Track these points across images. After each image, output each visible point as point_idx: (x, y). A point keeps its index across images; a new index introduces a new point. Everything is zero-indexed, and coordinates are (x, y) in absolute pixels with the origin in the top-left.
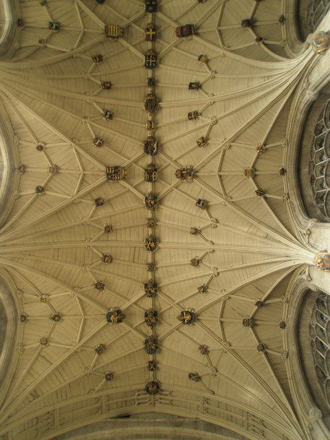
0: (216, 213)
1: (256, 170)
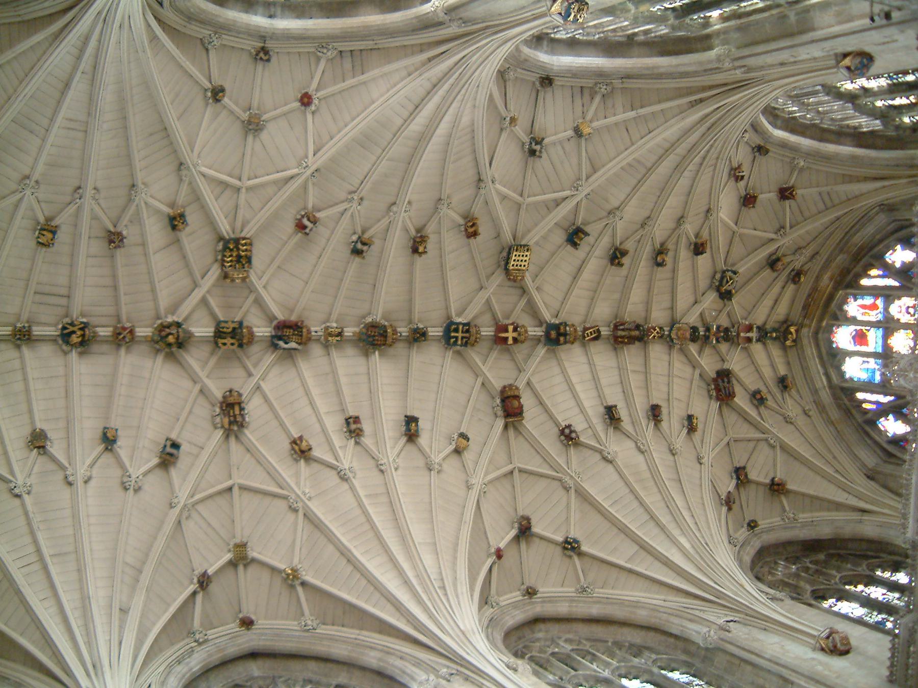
0: (154, 486)
1: (245, 566)
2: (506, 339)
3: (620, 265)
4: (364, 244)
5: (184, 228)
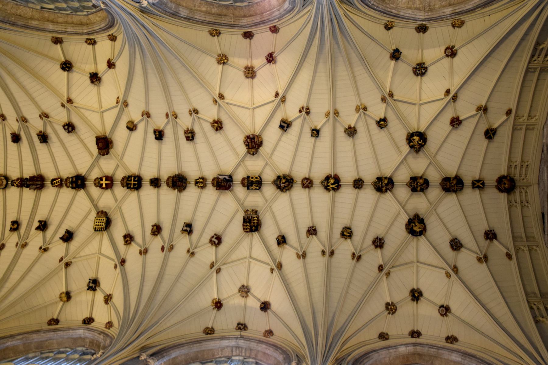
2: (106, 180)
3: (40, 221)
4: (186, 230)
5: (278, 237)
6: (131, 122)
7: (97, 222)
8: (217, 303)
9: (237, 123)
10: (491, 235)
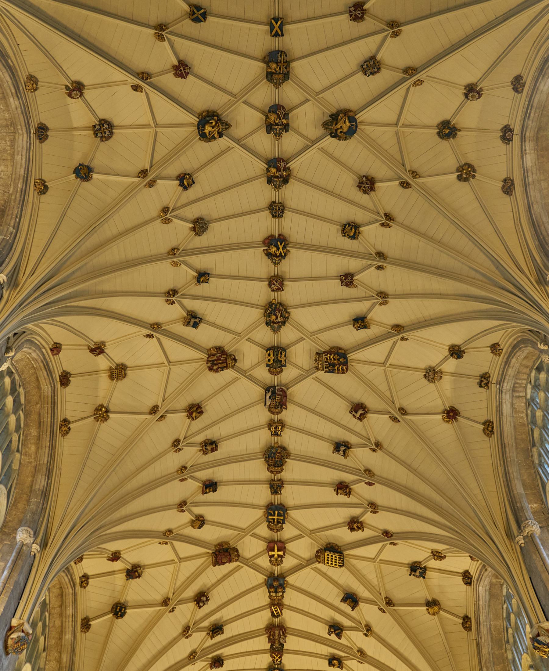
2: (273, 551)
3: (330, 633)
5: (355, 328)
6: (192, 524)
7: (332, 564)
8: (449, 417)
9: (192, 379)
10: (357, 13)
